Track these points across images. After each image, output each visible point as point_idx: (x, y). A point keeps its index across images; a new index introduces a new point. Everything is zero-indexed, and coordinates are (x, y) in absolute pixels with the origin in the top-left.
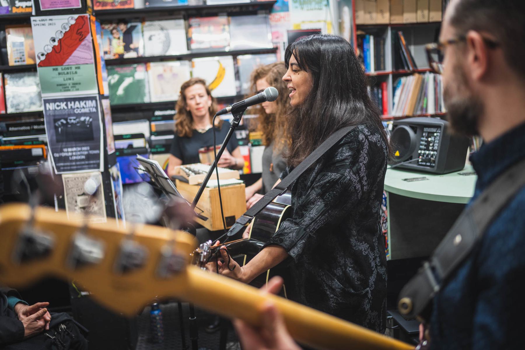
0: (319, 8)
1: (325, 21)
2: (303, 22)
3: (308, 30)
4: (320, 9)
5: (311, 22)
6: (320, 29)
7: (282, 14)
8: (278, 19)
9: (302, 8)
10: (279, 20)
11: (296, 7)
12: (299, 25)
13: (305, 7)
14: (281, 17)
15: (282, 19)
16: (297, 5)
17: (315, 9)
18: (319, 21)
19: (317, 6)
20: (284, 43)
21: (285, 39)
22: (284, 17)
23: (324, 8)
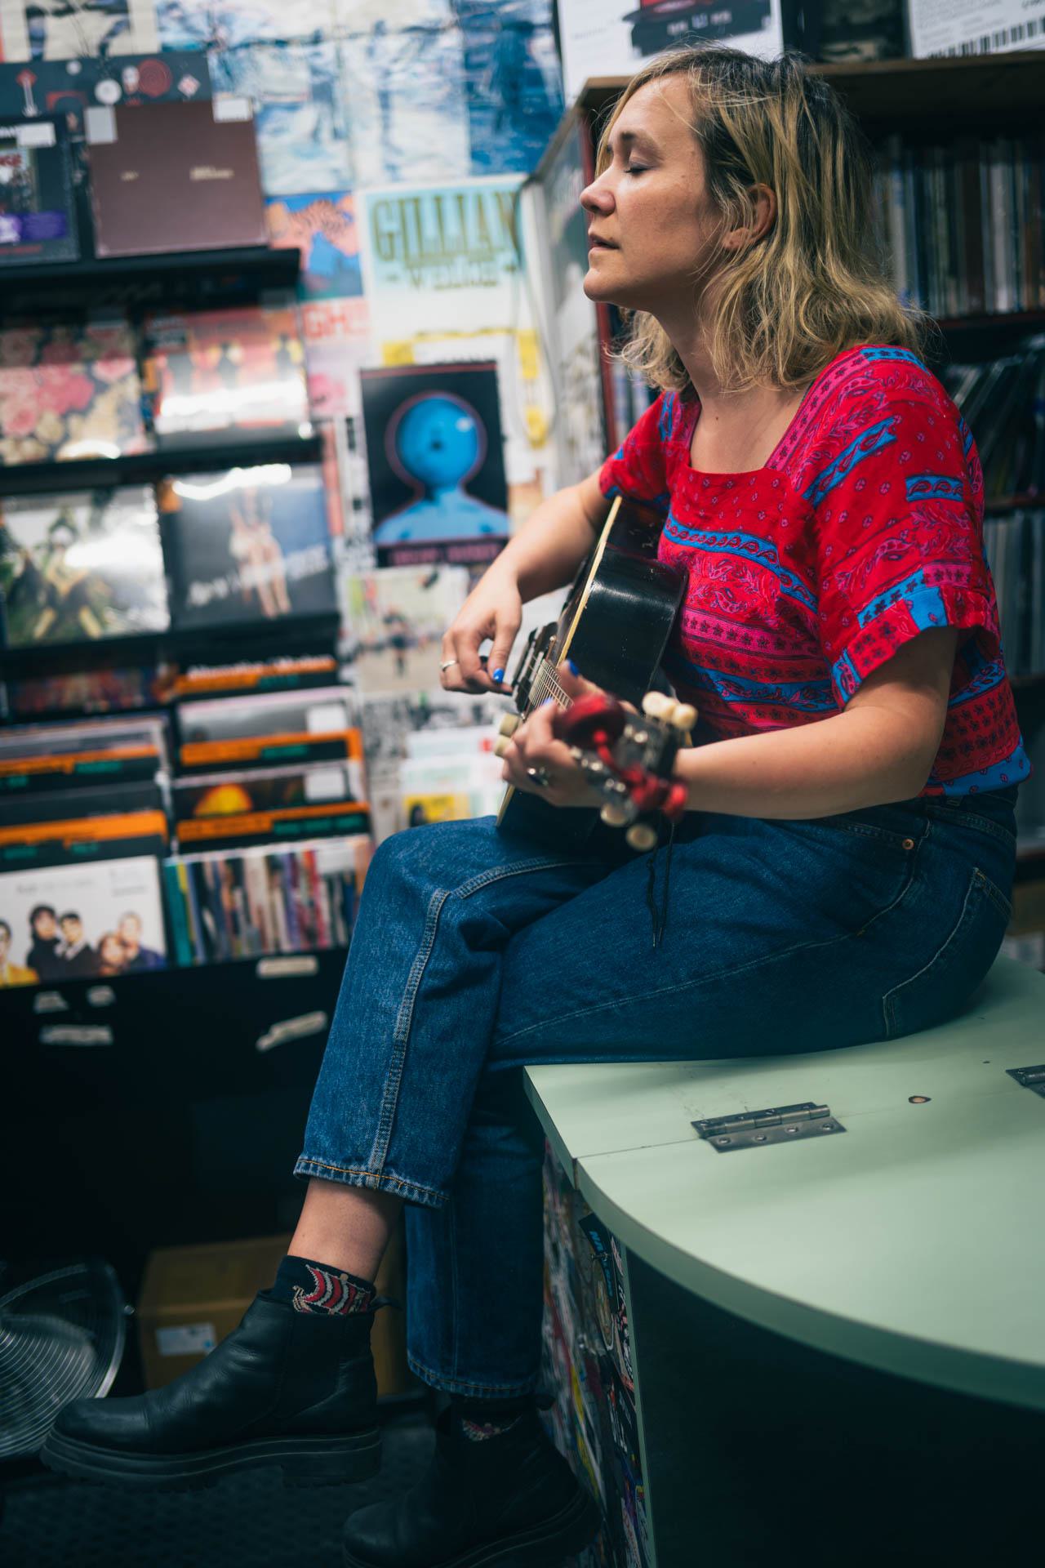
0: (485, 277)
1: (510, 331)
2: (422, 335)
3: (439, 365)
4: (491, 283)
5: (454, 334)
6: (492, 363)
7: (336, 305)
8: (319, 325)
9: (417, 282)
10: (323, 331)
11: (393, 278)
12: (405, 348)
13: (428, 275)
14: (333, 320)
15: (339, 327)
16: (396, 267)
17: (470, 283)
18: (486, 331)
19: (475, 272)
20: (349, 421)
21: (353, 405)
22: (343, 318)
23: (505, 278)
